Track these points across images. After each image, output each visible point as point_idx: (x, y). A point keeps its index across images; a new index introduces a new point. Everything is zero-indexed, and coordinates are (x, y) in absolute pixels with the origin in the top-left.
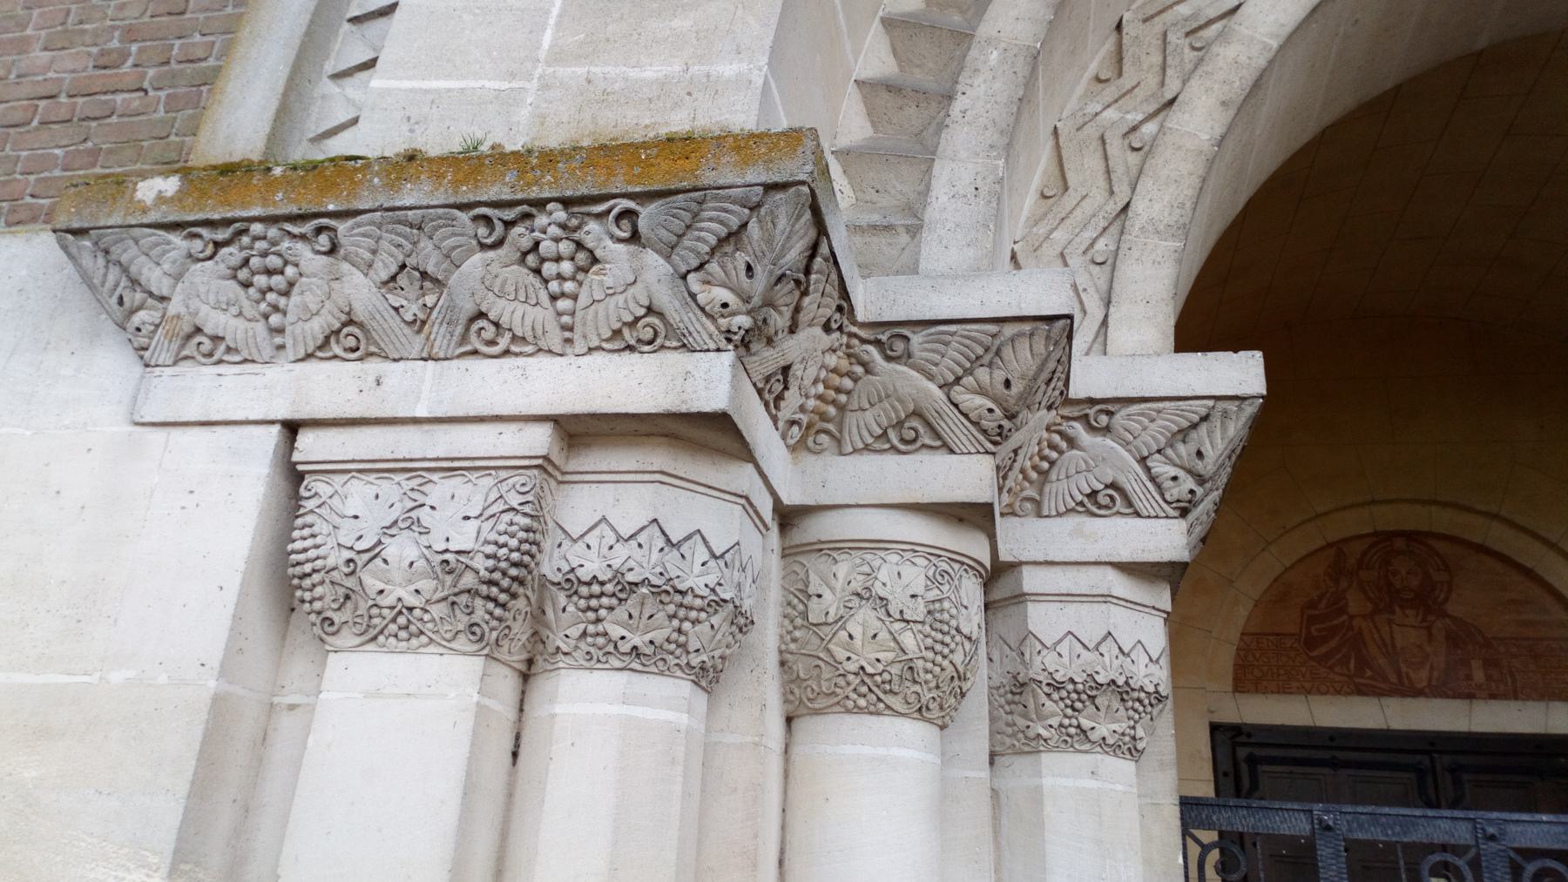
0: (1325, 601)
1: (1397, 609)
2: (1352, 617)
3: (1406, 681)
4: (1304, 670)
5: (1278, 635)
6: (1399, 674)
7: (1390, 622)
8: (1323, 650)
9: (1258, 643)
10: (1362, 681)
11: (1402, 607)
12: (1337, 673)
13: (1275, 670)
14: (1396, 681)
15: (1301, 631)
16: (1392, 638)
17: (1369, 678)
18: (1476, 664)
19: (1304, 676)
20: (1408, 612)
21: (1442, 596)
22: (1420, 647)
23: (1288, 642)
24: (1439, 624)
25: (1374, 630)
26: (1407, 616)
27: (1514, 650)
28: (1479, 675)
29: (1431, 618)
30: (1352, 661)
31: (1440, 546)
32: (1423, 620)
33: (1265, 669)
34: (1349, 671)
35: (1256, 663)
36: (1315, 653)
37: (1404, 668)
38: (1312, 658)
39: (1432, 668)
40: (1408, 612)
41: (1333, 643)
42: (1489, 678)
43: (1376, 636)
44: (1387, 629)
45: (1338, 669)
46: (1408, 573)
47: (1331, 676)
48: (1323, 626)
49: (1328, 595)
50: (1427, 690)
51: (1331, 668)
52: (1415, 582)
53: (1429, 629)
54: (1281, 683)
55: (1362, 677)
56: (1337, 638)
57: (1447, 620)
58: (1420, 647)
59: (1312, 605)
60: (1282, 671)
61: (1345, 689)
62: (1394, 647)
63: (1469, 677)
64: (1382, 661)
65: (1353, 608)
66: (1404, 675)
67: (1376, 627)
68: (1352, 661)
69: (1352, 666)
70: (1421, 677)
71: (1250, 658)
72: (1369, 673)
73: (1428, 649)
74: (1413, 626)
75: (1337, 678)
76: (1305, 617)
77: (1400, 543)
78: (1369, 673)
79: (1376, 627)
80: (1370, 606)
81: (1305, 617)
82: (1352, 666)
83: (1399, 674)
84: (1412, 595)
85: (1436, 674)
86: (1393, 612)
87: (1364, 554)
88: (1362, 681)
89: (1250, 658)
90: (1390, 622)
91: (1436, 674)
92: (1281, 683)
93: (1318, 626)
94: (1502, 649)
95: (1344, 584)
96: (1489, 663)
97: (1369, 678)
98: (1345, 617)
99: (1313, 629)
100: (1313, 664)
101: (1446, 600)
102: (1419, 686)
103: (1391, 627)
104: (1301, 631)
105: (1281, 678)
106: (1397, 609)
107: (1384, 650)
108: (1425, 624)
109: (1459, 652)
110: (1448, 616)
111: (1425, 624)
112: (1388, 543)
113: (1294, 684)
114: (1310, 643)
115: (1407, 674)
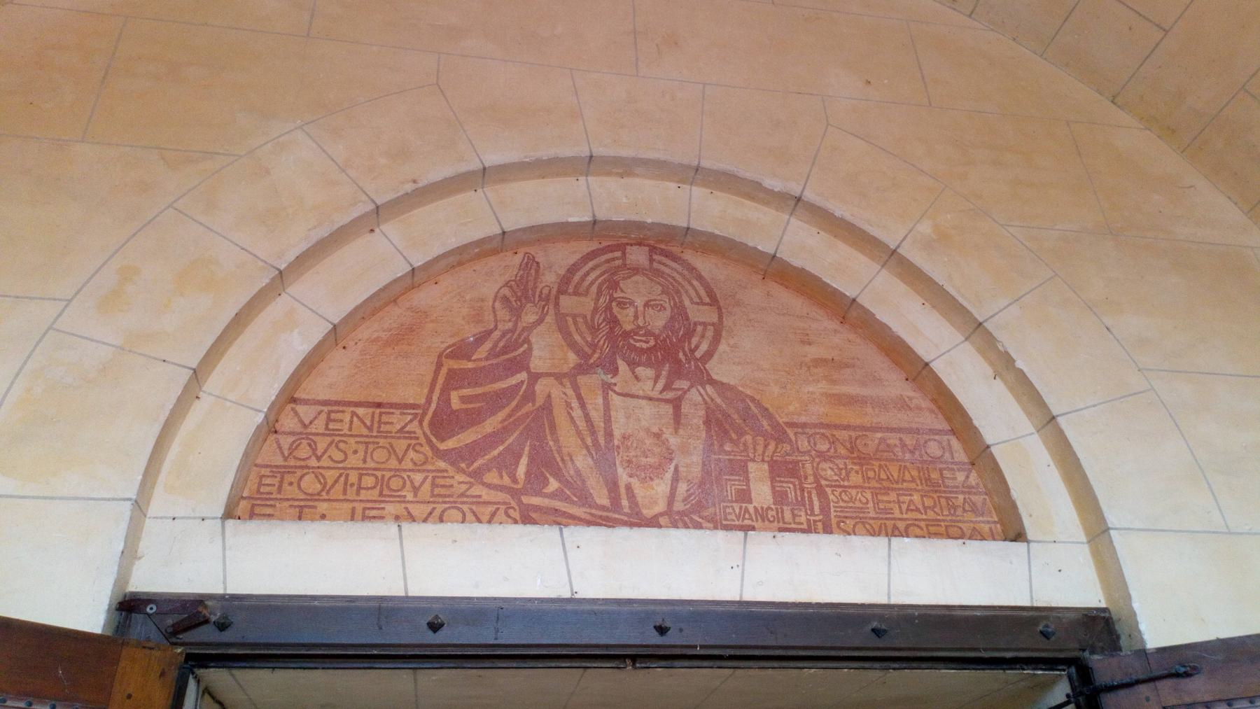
0: (488, 345)
1: (622, 366)
2: (534, 377)
3: (625, 503)
4: (418, 478)
5: (379, 405)
6: (613, 487)
7: (607, 387)
8: (467, 437)
9: (329, 420)
10: (536, 501)
11: (632, 365)
12: (489, 486)
13: (353, 478)
14: (605, 501)
15: (429, 401)
16: (608, 420)
17: (553, 496)
18: (758, 471)
19: (416, 490)
20: (640, 370)
21: (704, 347)
22: (658, 436)
23: (397, 420)
24: (694, 395)
25: (575, 404)
26: (637, 378)
27: (823, 446)
28: (762, 493)
29: (684, 384)
30: (524, 461)
31: (705, 265)
32: (667, 387)
33: (331, 475)
34: (515, 480)
35: (313, 462)
36: (450, 444)
37: (623, 476)
38: (442, 455)
39: (676, 479)
40: (645, 372)
41: (490, 425)
42: (780, 497)
43: (577, 413)
44: (600, 400)
45: (492, 477)
46: (646, 305)
47: (477, 490)
48: (479, 390)
49: (497, 334)
50: (662, 520)
51: (477, 475)
52: (658, 321)
53: (676, 404)
54: (359, 507)
55: (539, 493)
56: (501, 415)
57: (709, 388)
58: (658, 436)
59: (460, 351)
60: (368, 481)
61: (501, 515)
62: (609, 435)
63: (744, 496)
64: (583, 462)
65: (539, 361)
66: (623, 491)
67: (580, 398)
68: (524, 461)
69: (521, 470)
70: (654, 494)
71: (304, 452)
72: (554, 485)
73: (673, 441)
74: (651, 399)
75: (486, 494)
76: (444, 371)
77: (637, 256)
78: (554, 485)
79: (580, 398)
80: (572, 358)
81: (444, 371)
82: (521, 470)
83: (613, 487)
84: (652, 343)
85: (682, 488)
86: (615, 372)
87: (573, 270)
88: (536, 501)
89: (304, 452)
90: (607, 387)
91: (682, 488)
92: (359, 507)
93: (466, 392)
94: (804, 444)
95: (529, 317)
96: (782, 470)
97: (553, 496)
98: (523, 376)
99: (455, 397)
100: (442, 464)
101: (709, 354)
102: (648, 513)
103: (606, 398)
104: (429, 401)
105: (364, 495)
106: (622, 366)
107: (589, 441)
108: (669, 395)
109: (728, 447)
110: (712, 382)
111: (669, 395)
112: (618, 254)
113: (391, 508)
114: (444, 423)
115: (629, 488)
